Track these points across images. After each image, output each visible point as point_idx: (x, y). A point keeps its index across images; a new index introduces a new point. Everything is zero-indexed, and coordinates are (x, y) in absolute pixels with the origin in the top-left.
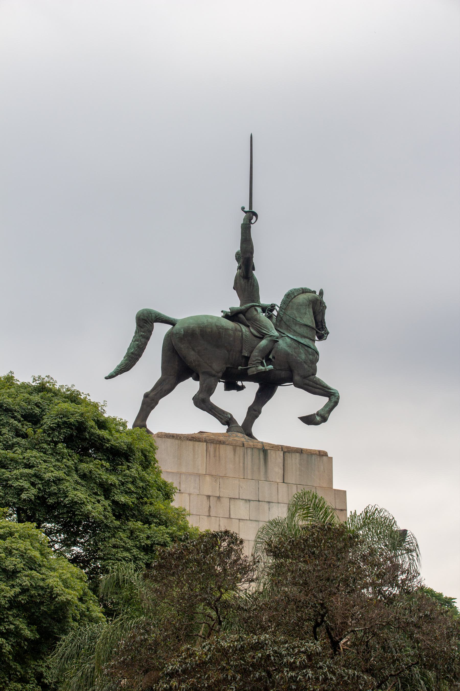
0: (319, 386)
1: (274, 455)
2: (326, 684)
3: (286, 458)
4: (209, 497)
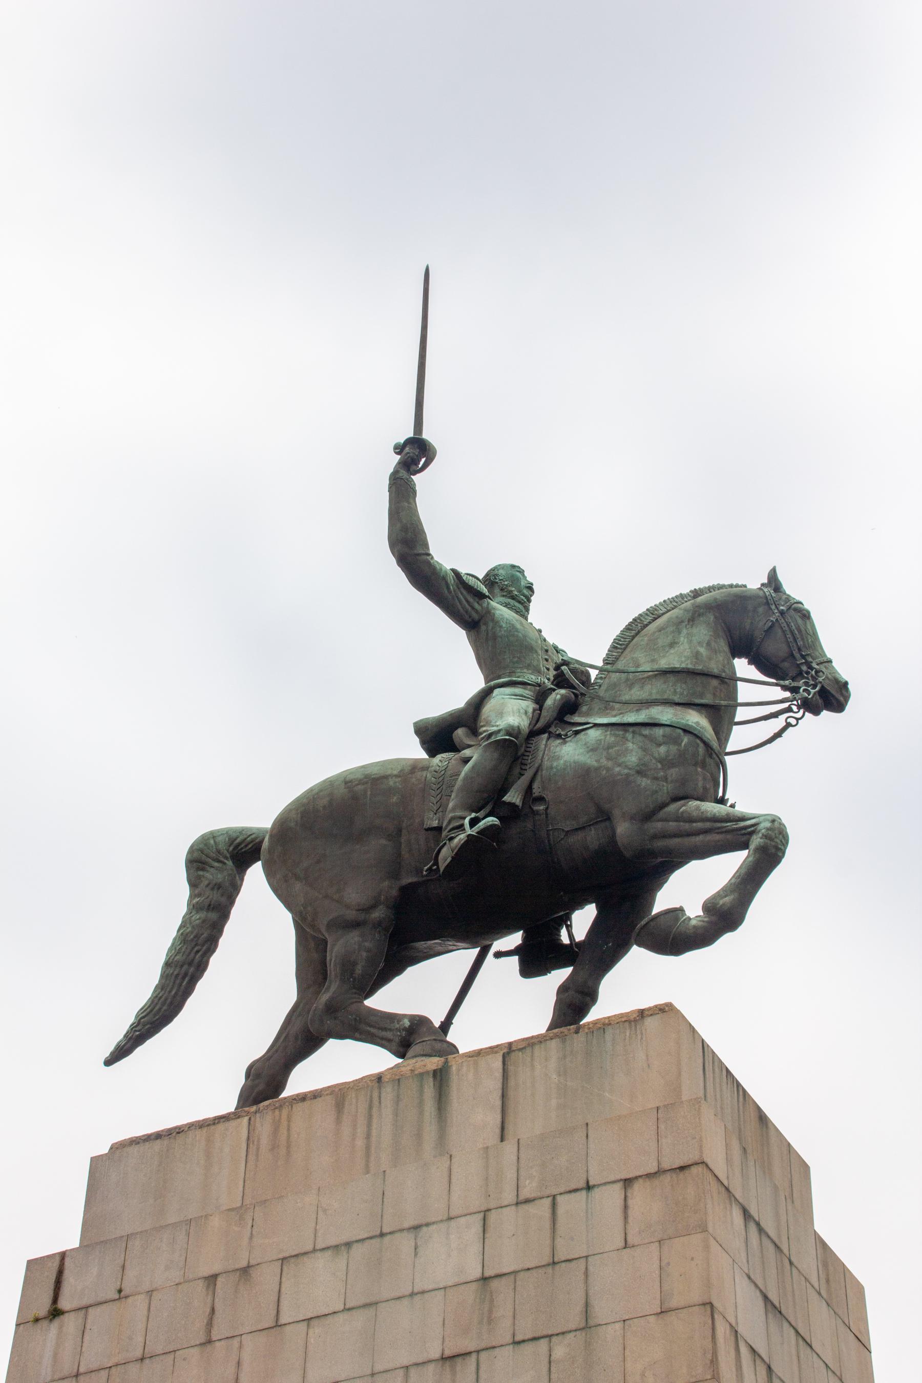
0: (700, 825)
1: (471, 1076)
3: (511, 1068)
4: (212, 1279)
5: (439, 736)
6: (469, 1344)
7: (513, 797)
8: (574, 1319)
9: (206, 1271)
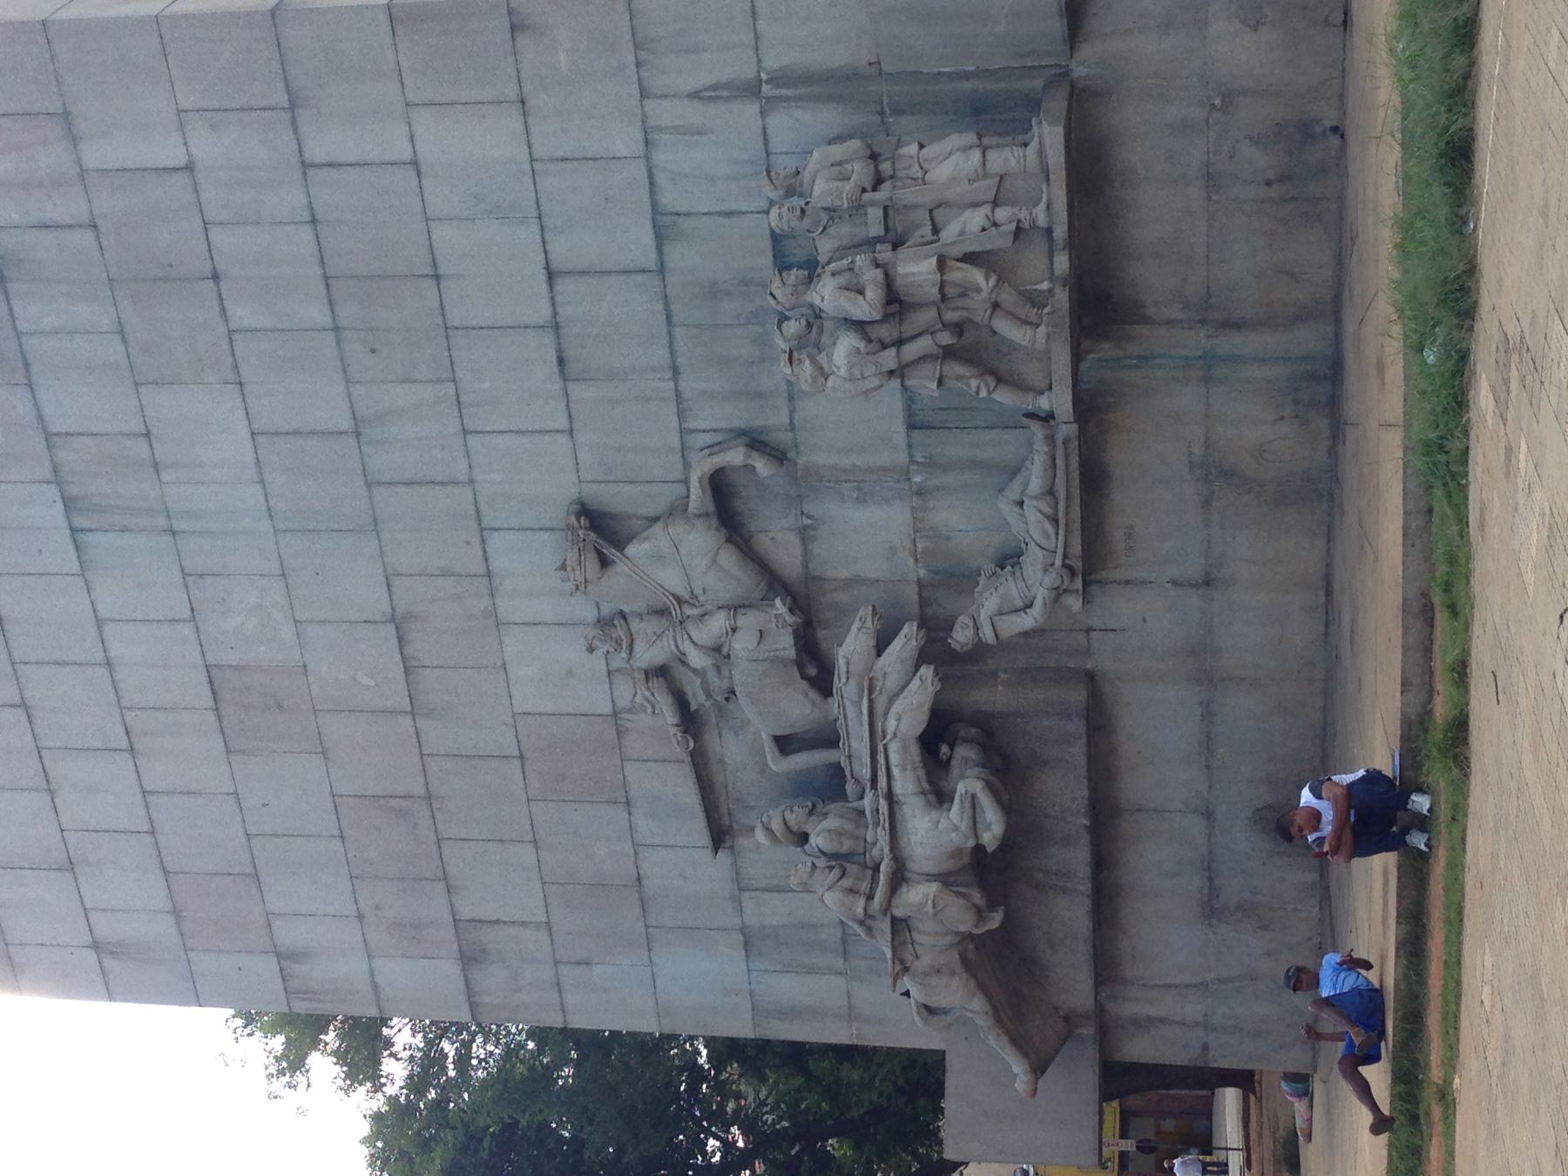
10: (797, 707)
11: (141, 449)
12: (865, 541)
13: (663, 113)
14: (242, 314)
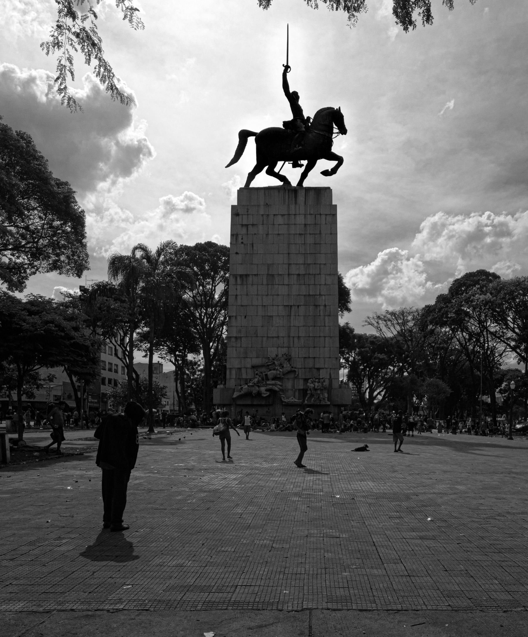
2: (179, 279)
4: (262, 215)
5: (285, 124)
6: (303, 233)
7: (303, 143)
8: (318, 233)
9: (261, 213)
10: (270, 377)
11: (297, 315)
12: (289, 385)
13: (329, 370)
14: (311, 328)
